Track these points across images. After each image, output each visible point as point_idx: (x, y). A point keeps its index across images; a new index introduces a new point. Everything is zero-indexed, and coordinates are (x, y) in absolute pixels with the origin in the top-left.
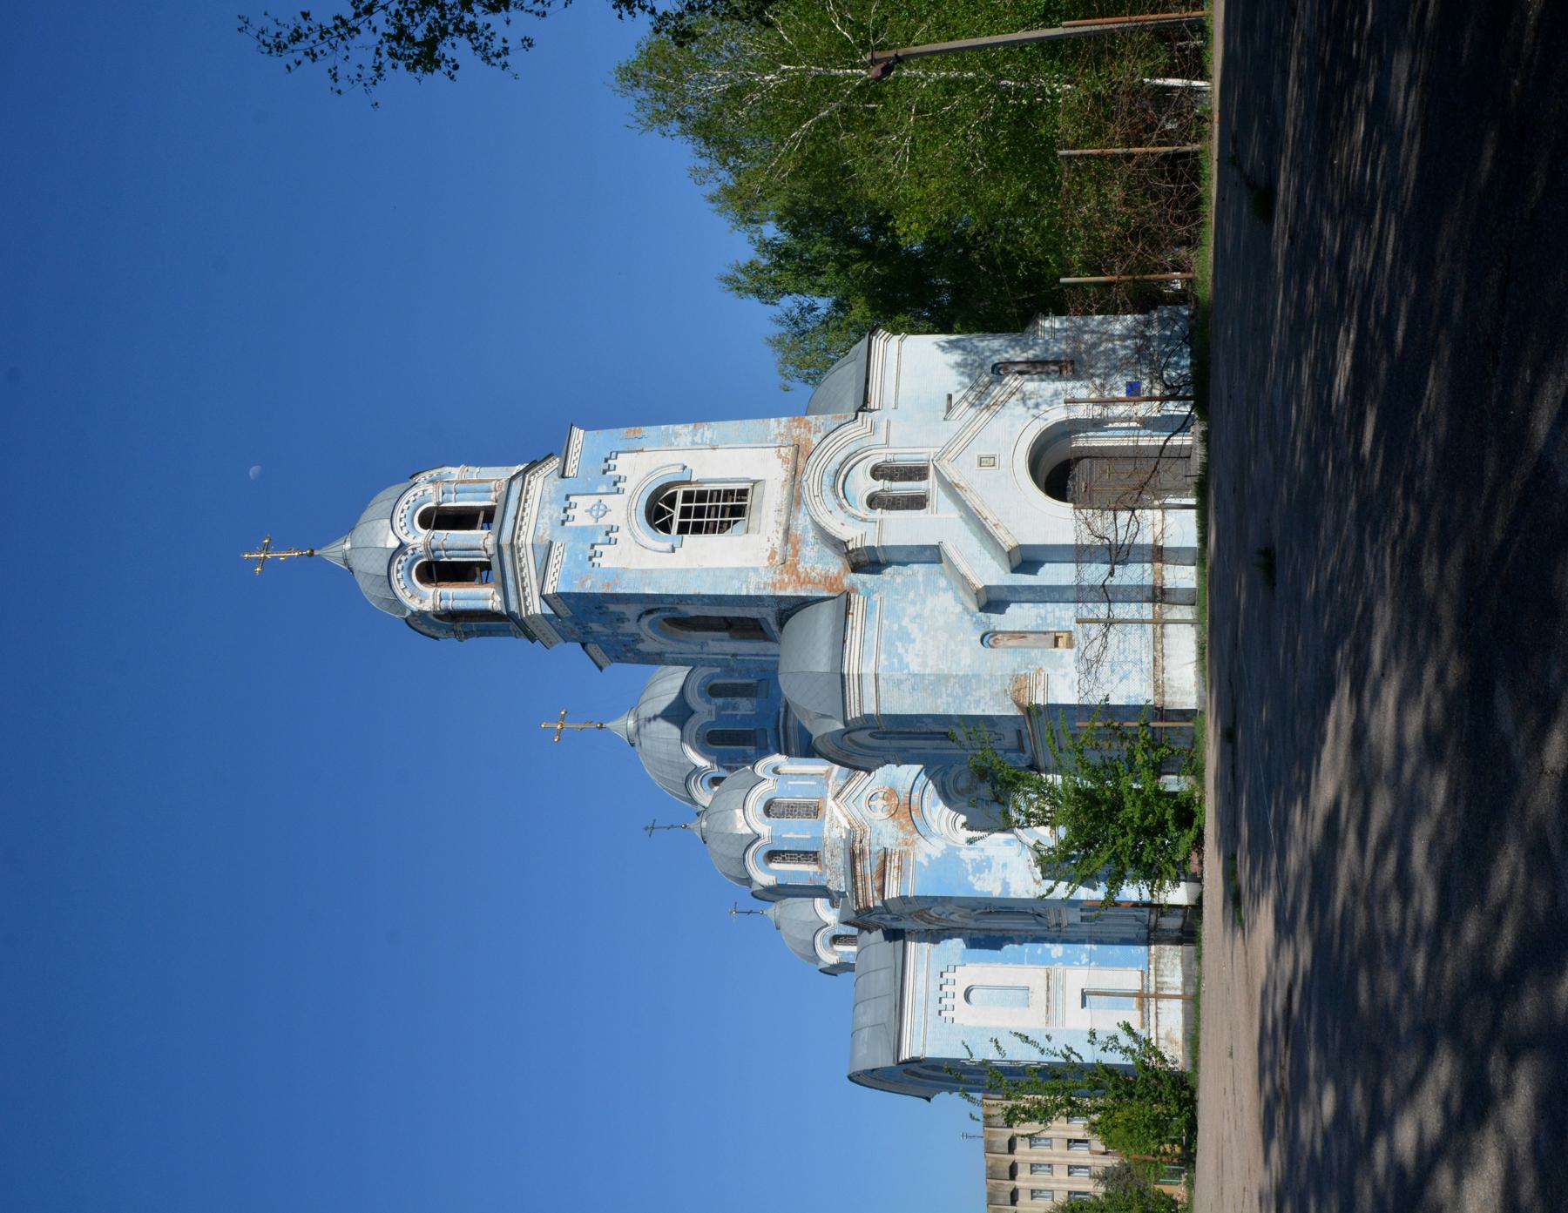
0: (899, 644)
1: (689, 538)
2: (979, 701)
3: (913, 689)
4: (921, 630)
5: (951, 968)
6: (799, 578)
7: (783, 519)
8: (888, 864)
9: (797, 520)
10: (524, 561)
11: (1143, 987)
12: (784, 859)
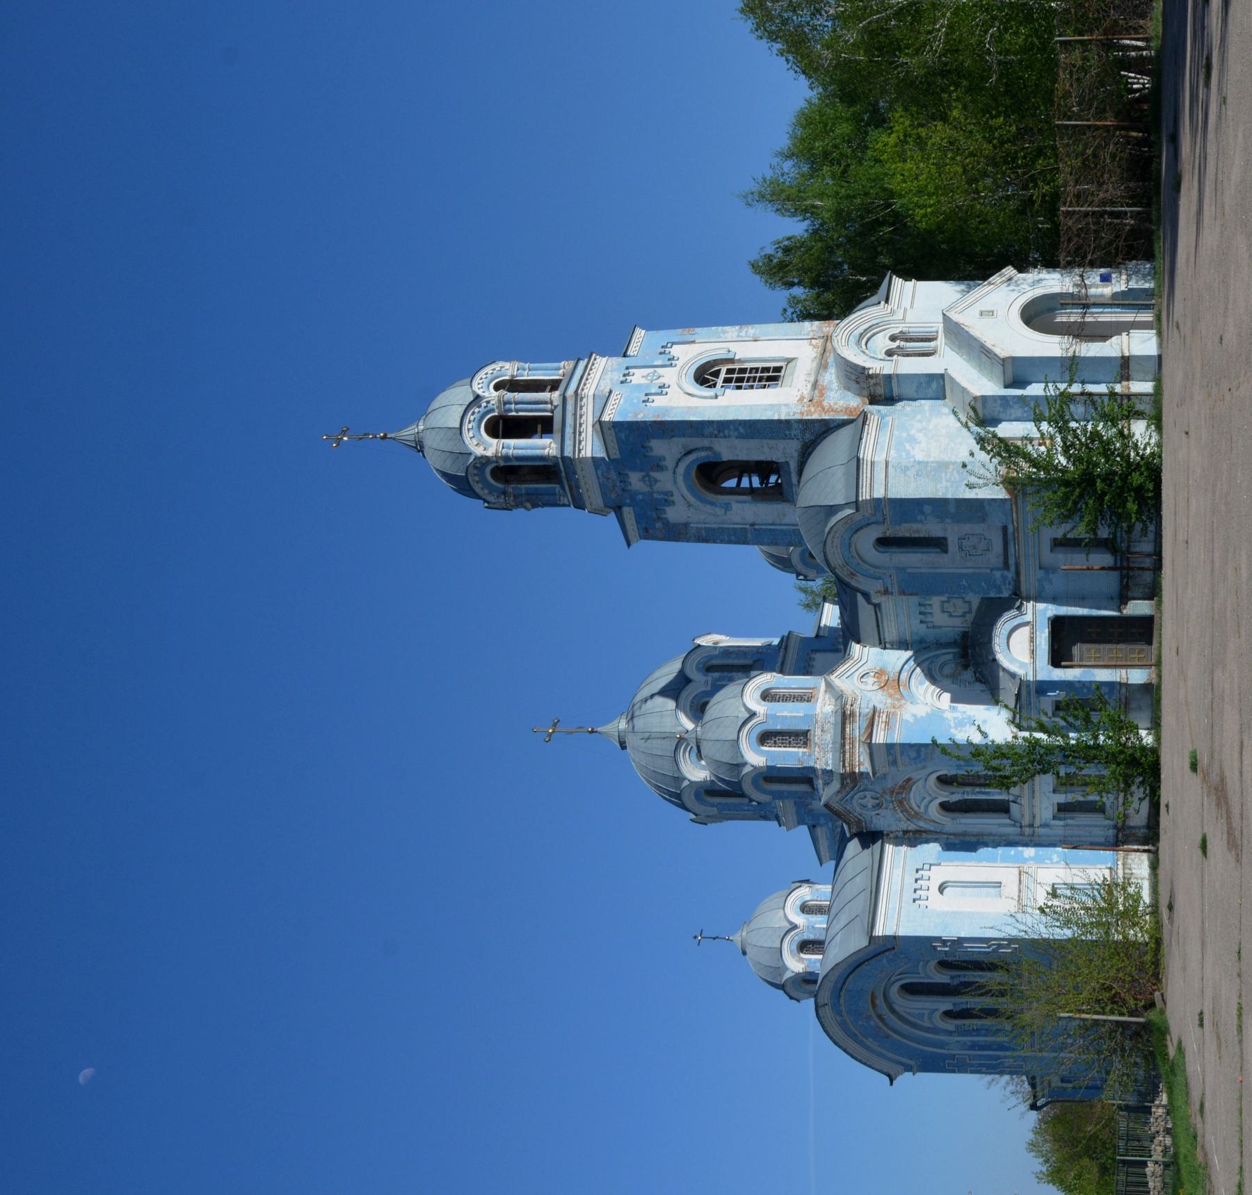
5: (927, 867)
6: (823, 409)
8: (877, 718)
10: (584, 409)
12: (775, 742)
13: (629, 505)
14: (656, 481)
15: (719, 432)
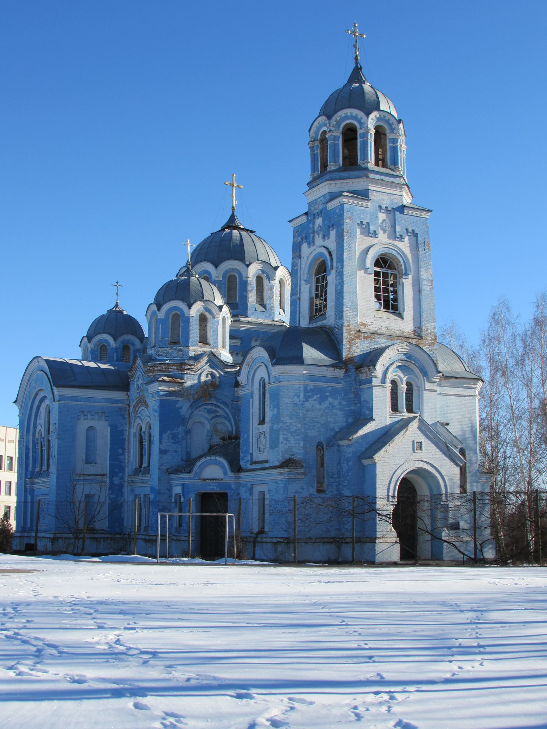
0: (318, 396)
1: (372, 277)
2: (287, 440)
3: (294, 404)
4: (326, 408)
6: (353, 340)
7: (383, 331)
9: (383, 338)
11: (97, 530)
13: (307, 219)
14: (318, 234)
15: (338, 273)
